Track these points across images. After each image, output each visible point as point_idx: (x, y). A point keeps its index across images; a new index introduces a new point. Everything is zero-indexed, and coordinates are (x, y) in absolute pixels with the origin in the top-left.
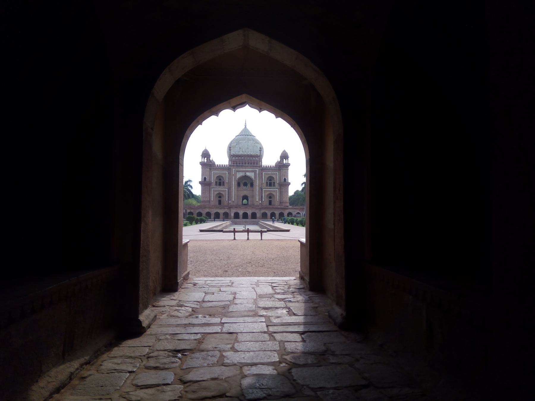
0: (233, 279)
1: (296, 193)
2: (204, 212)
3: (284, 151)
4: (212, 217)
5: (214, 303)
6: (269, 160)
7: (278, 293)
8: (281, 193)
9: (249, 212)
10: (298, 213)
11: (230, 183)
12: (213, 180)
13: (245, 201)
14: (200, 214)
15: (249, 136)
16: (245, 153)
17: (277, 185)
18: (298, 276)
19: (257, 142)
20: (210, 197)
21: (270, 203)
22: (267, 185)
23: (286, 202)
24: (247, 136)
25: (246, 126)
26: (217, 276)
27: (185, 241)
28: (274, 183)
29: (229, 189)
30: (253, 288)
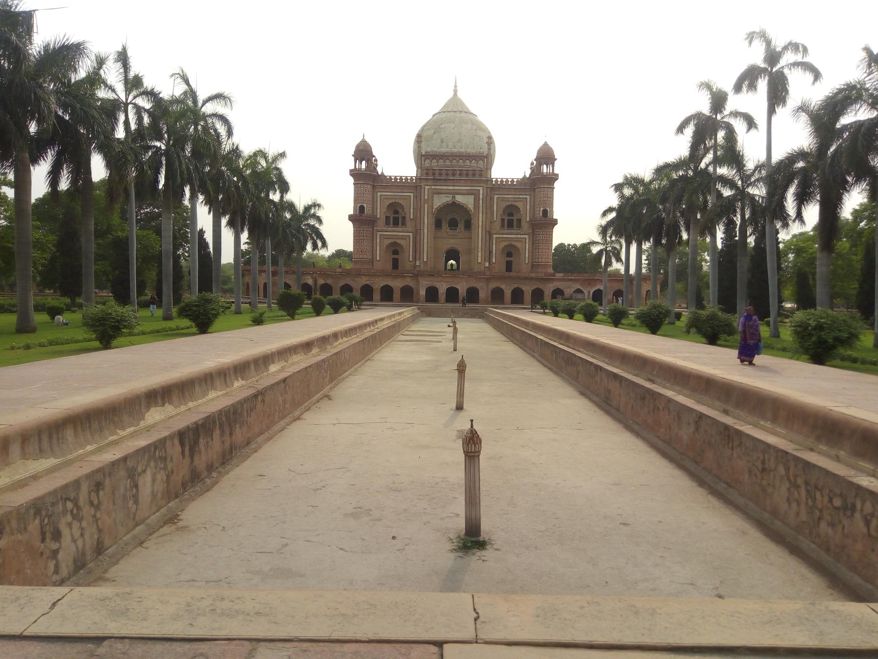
2: (357, 284)
3: (546, 144)
4: (377, 296)
6: (510, 165)
8: (534, 243)
9: (462, 288)
10: (579, 291)
11: (418, 219)
12: (380, 212)
14: (346, 289)
15: (463, 115)
16: (456, 150)
17: (525, 226)
19: (480, 127)
21: (509, 267)
22: (503, 226)
23: (545, 266)
28: (519, 221)
29: (417, 233)
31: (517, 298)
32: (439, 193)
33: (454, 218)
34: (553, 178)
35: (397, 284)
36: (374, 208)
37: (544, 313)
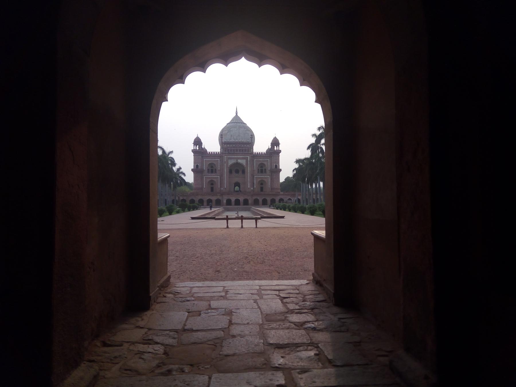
0: (228, 284)
1: (287, 179)
2: (197, 199)
4: (205, 203)
5: (200, 335)
6: (261, 146)
7: (292, 312)
8: (272, 179)
10: (290, 199)
13: (237, 188)
14: (192, 201)
15: (240, 124)
16: (237, 141)
17: (268, 172)
18: (312, 278)
20: (202, 184)
21: (262, 189)
22: (258, 172)
24: (238, 124)
25: (237, 113)
26: (206, 279)
27: (161, 236)
28: (265, 170)
29: (222, 176)
30: (255, 301)
31: (264, 203)
32: (231, 159)
33: (237, 169)
34: (280, 151)
35: (214, 198)
36: (202, 165)
37: (274, 209)
